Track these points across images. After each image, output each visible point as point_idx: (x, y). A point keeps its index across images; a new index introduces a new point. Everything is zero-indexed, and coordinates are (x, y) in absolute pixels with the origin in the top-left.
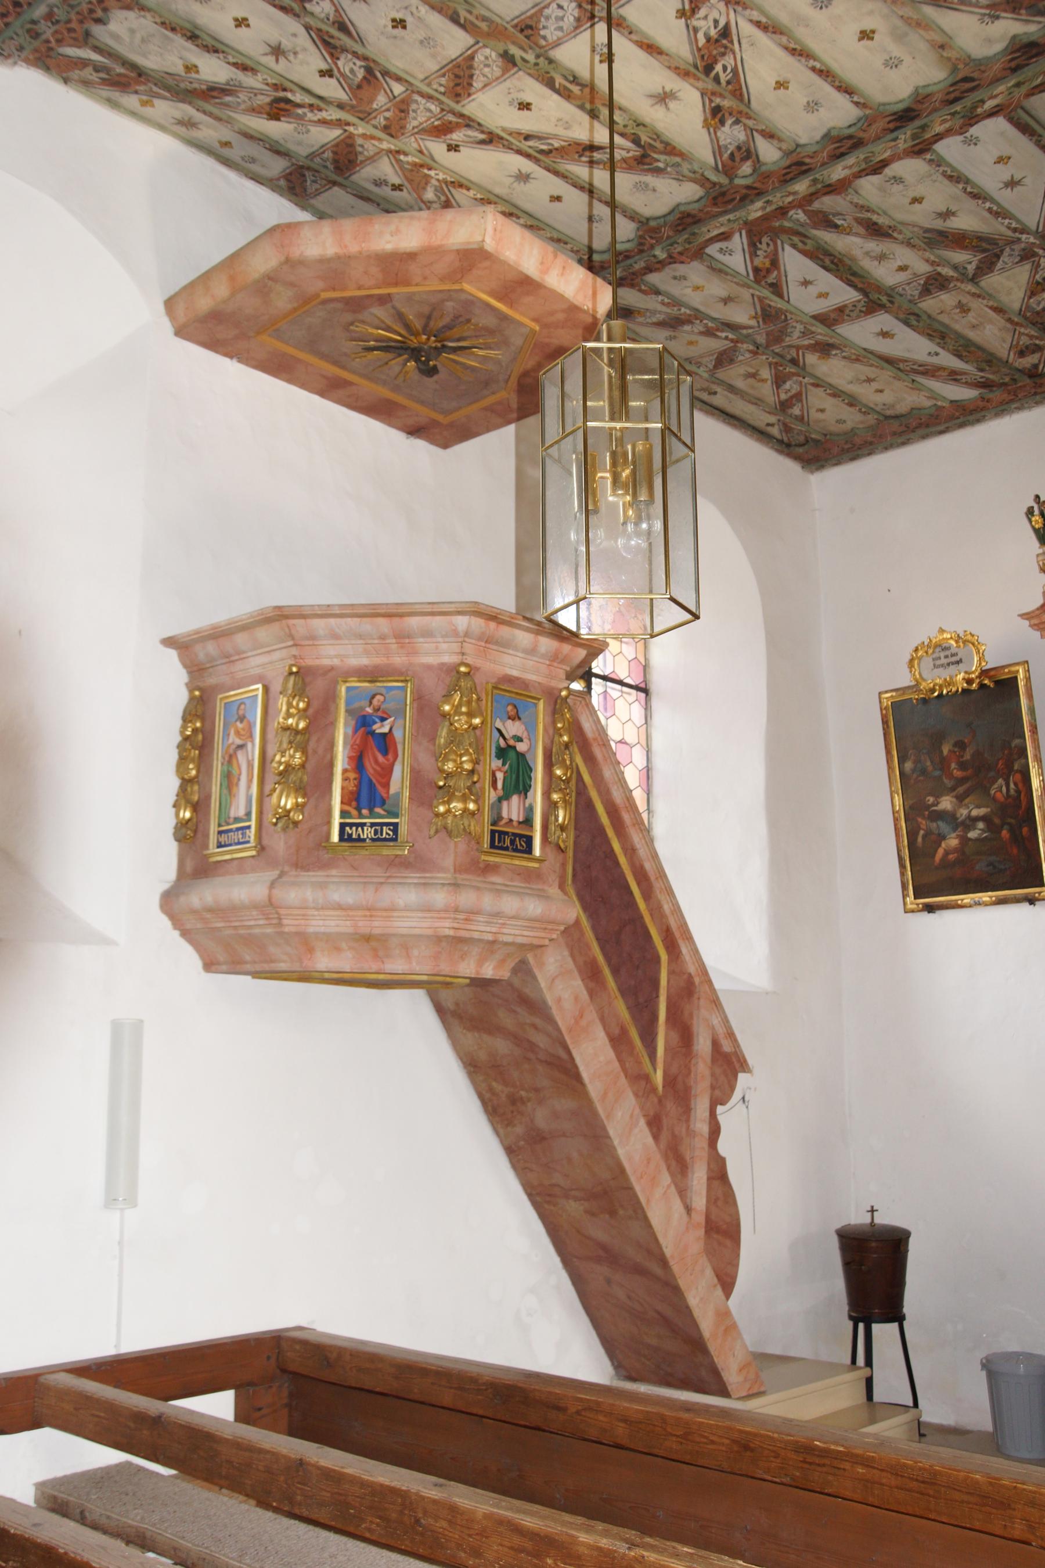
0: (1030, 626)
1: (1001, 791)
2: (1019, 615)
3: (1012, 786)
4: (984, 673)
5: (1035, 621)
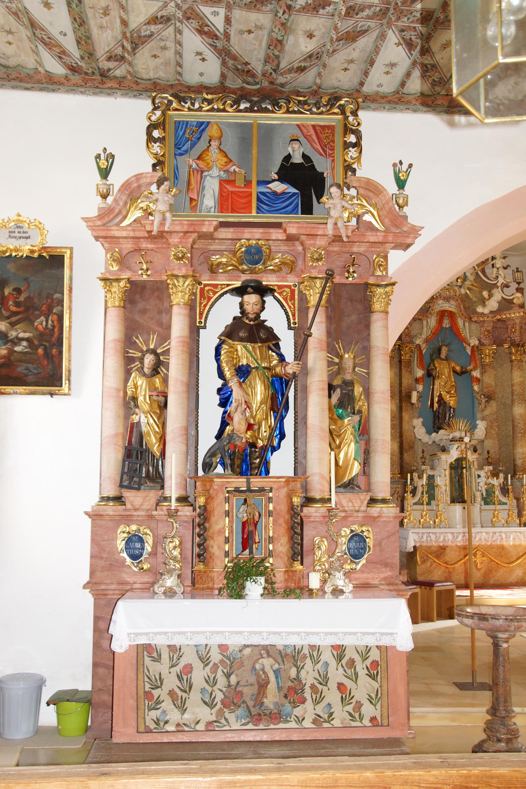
0: (87, 226)
1: (42, 324)
2: (82, 218)
3: (50, 322)
4: (44, 248)
5: (91, 224)
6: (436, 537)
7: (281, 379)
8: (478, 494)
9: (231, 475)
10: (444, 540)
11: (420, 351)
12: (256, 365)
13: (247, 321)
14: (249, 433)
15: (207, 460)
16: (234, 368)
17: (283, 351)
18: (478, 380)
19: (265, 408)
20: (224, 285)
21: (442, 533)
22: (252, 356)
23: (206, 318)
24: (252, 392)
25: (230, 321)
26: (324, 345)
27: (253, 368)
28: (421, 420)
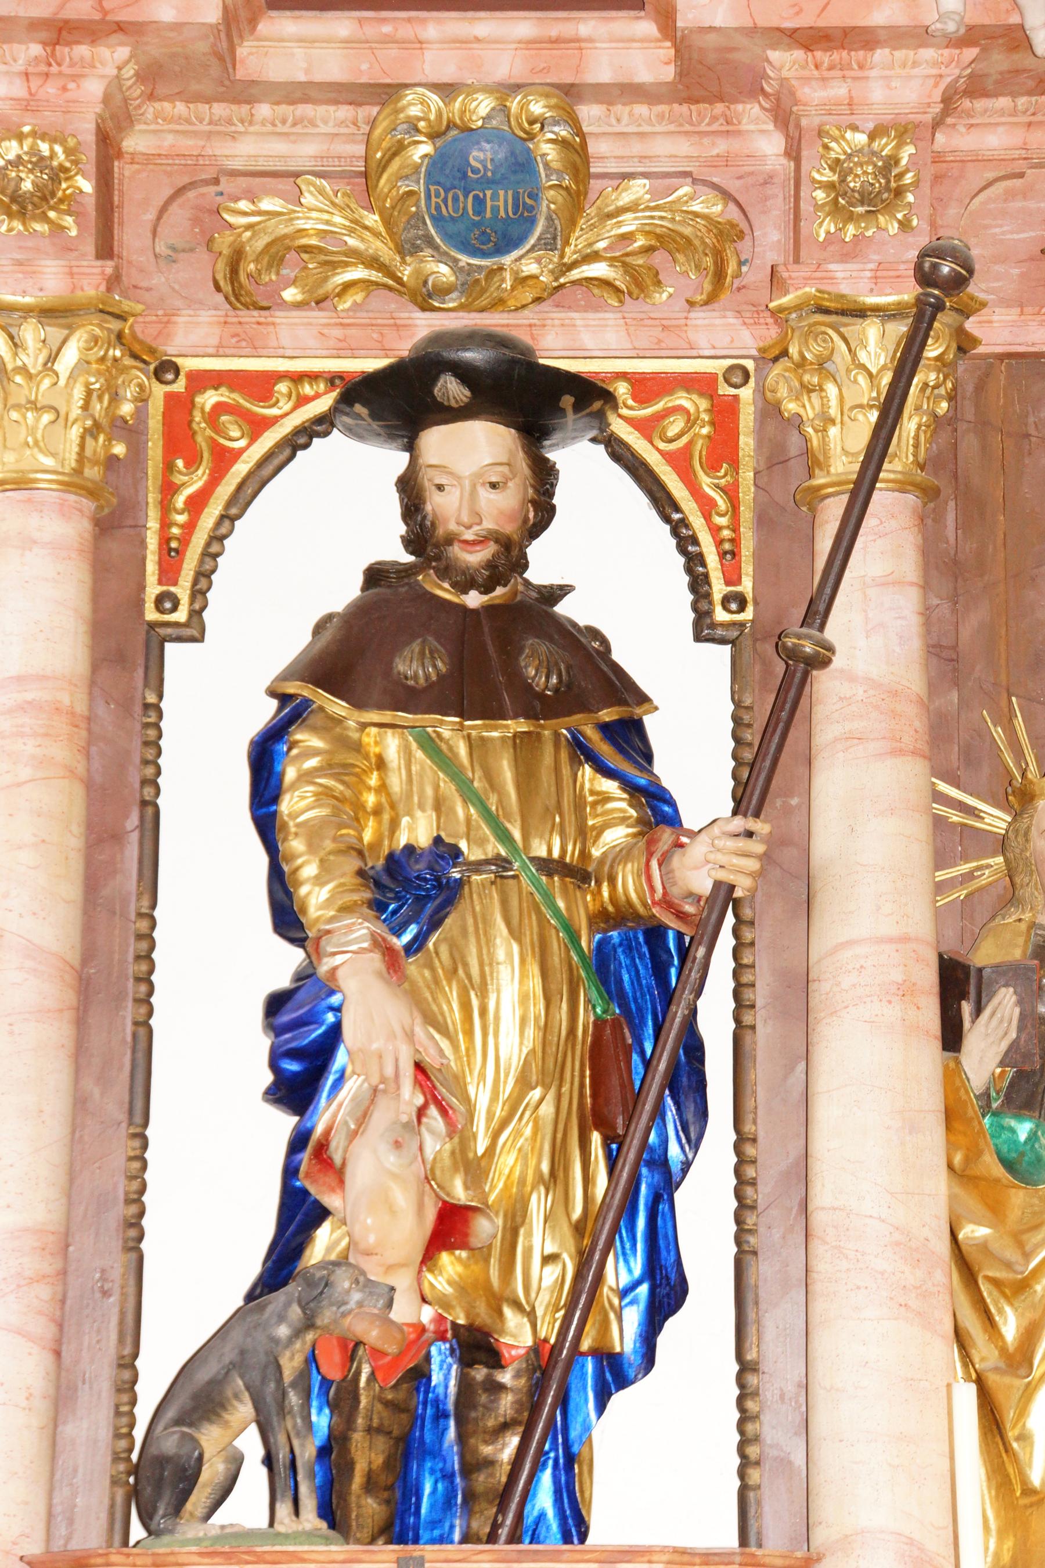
7: (655, 933)
9: (310, 1536)
12: (495, 848)
13: (445, 592)
14: (450, 1264)
15: (169, 1444)
16: (353, 864)
17: (668, 770)
19: (547, 1109)
20: (313, 377)
22: (468, 794)
23: (204, 576)
24: (466, 1006)
25: (344, 591)
26: (913, 726)
27: (478, 866)
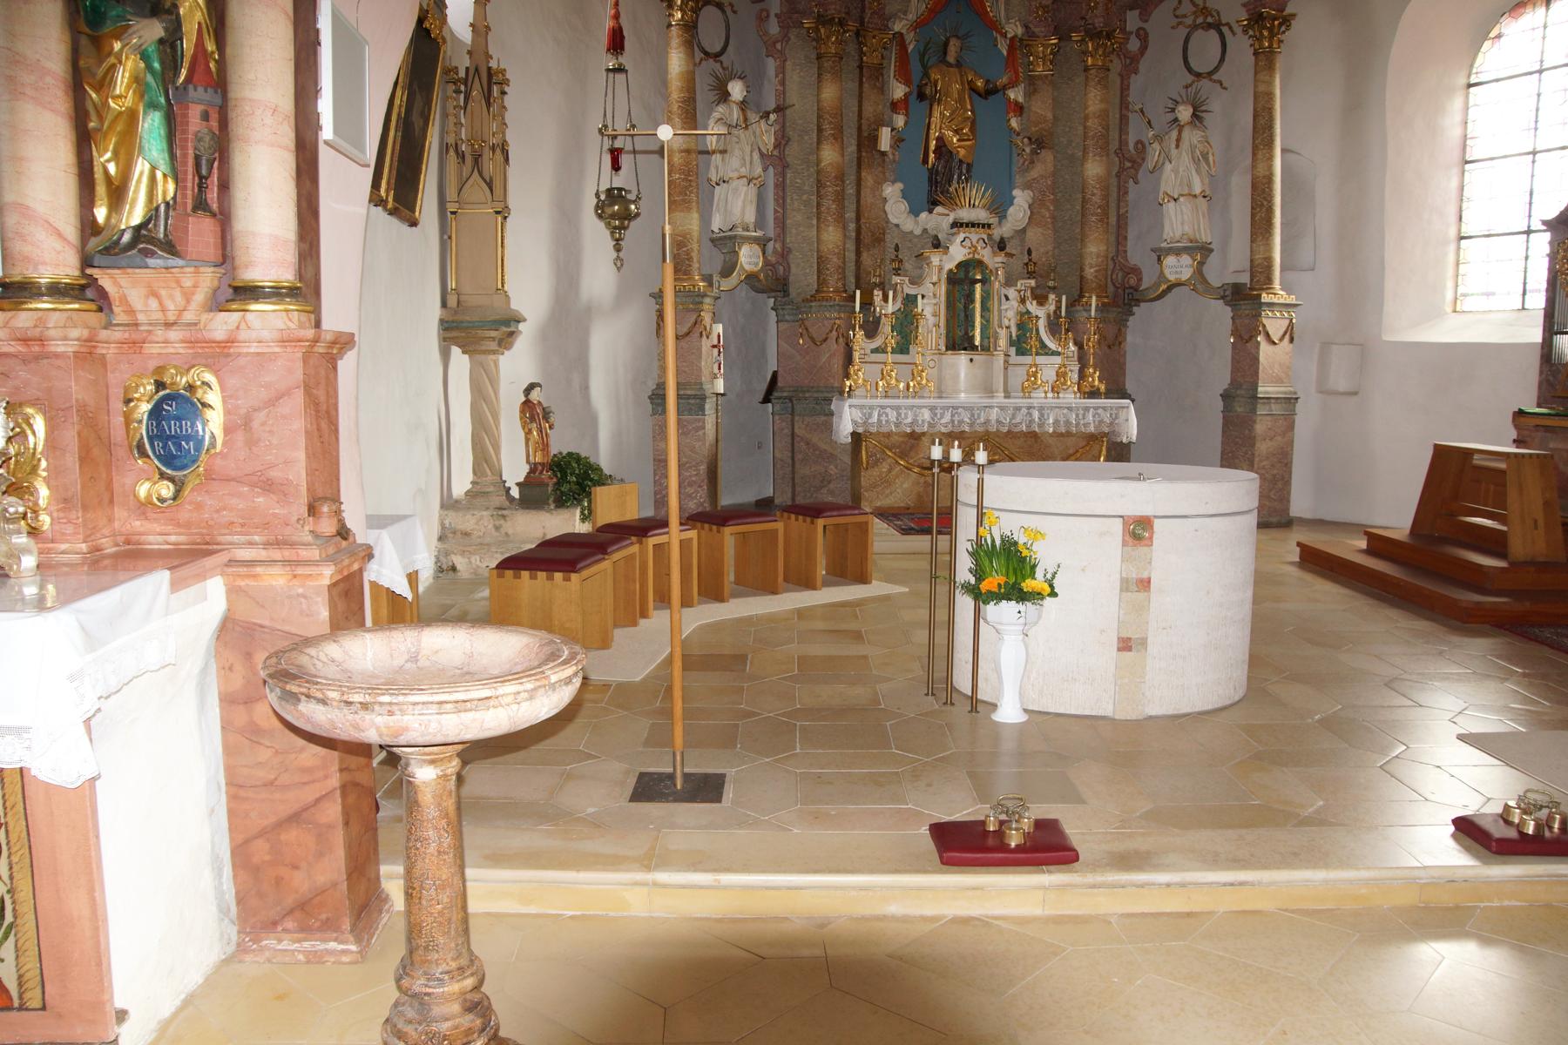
6: (899, 415)
8: (1003, 333)
10: (915, 422)
11: (903, 46)
18: (1019, 109)
21: (912, 407)
28: (900, 186)
